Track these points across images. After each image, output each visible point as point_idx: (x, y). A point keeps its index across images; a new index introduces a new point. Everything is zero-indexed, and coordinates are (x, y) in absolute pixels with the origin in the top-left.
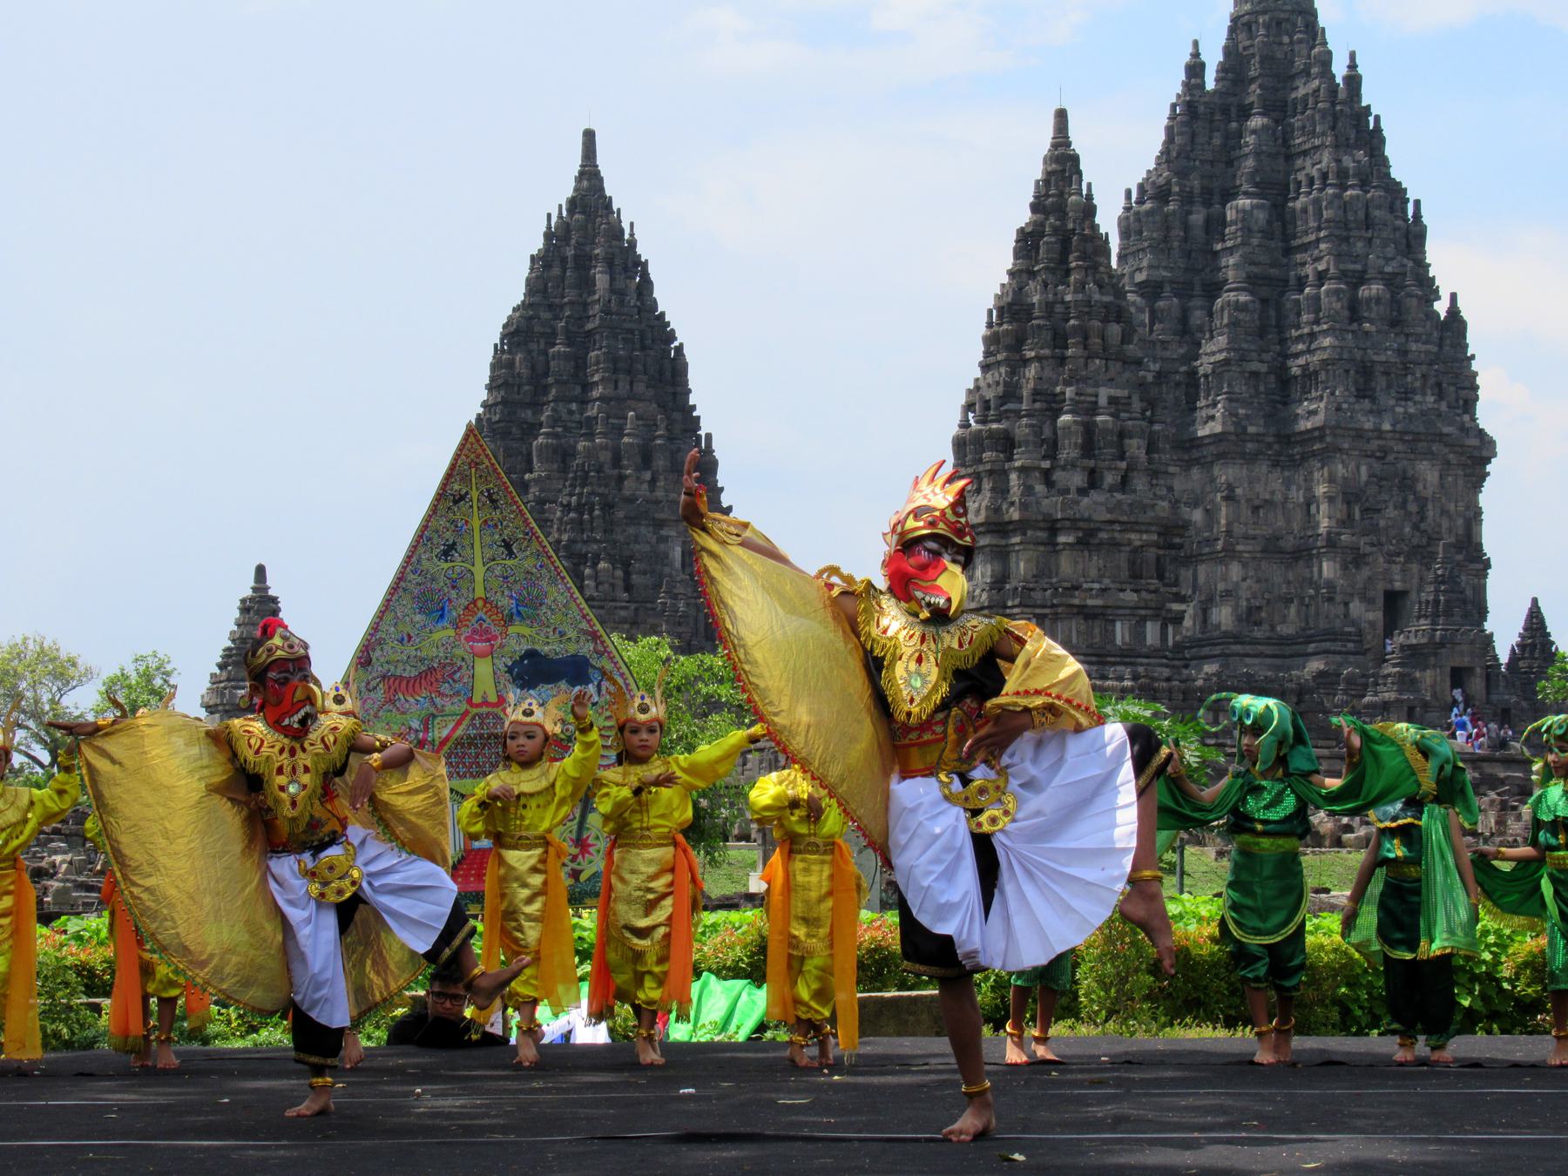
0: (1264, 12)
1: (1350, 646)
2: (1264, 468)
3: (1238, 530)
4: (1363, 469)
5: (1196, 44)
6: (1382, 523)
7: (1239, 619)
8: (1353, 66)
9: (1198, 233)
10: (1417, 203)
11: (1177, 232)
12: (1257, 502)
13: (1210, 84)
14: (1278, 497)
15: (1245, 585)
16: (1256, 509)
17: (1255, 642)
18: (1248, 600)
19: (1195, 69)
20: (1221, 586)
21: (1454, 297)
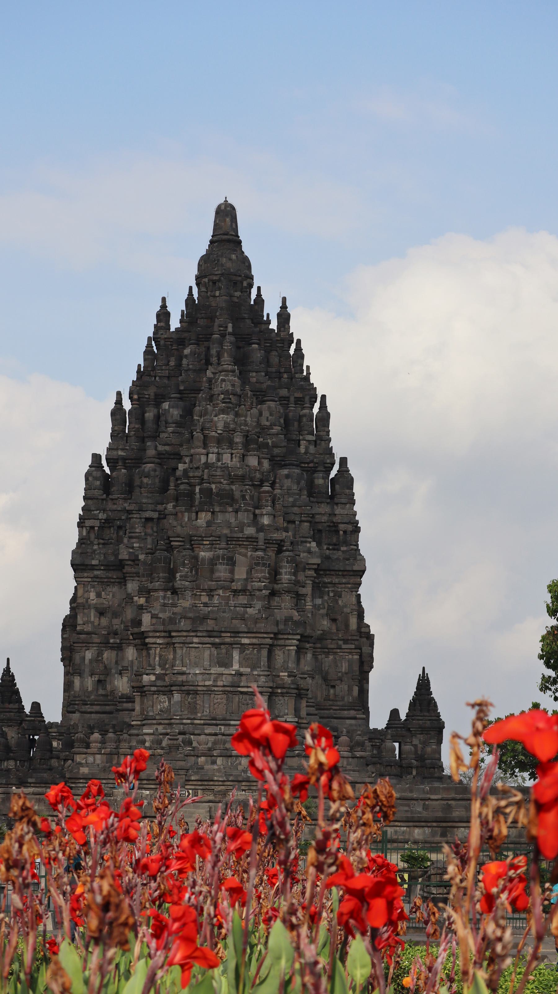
0: (205, 277)
5: (164, 299)
8: (284, 307)
9: (150, 425)
10: (324, 397)
13: (175, 323)
19: (163, 315)
21: (344, 461)
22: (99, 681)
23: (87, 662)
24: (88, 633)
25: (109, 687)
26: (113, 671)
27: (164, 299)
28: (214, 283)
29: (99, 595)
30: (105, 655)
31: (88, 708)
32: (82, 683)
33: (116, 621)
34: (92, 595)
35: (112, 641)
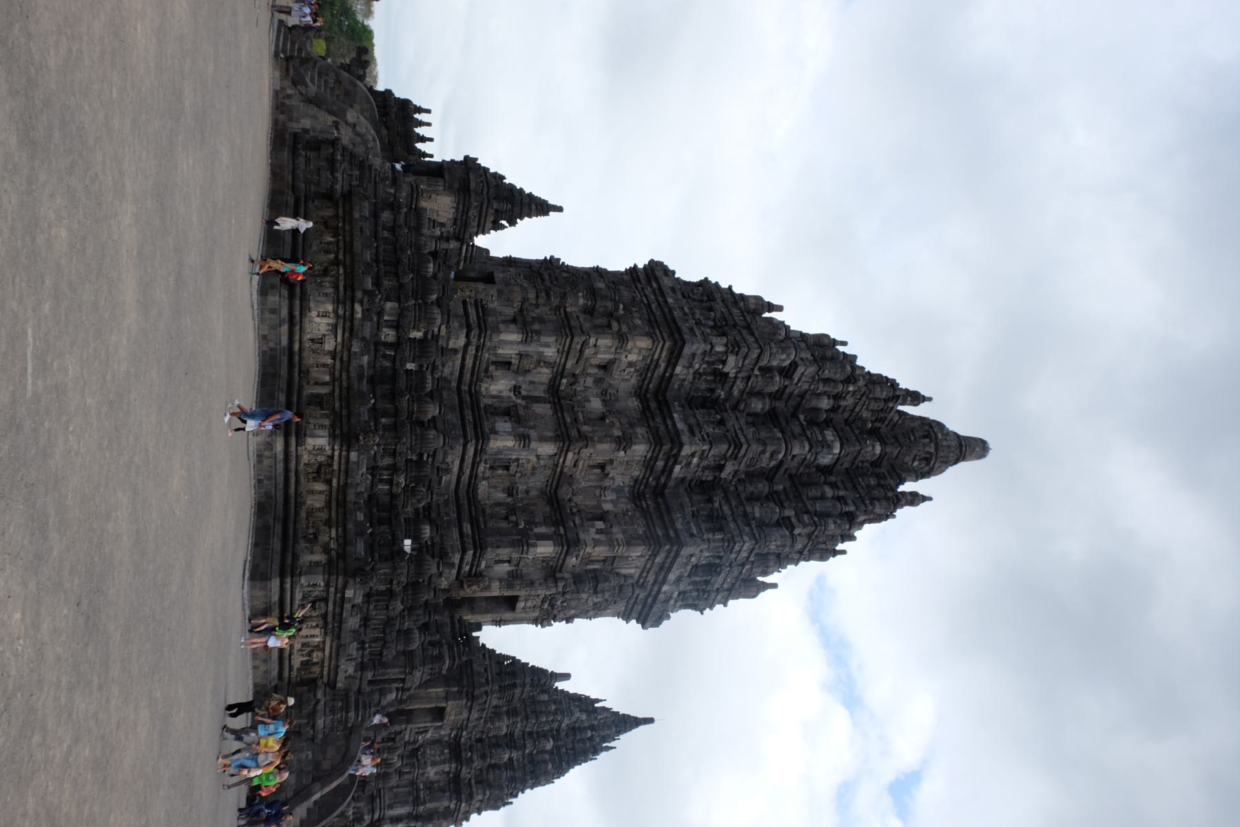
1: (467, 568)
2: (636, 473)
3: (586, 452)
4: (632, 571)
5: (930, 399)
6: (584, 596)
7: (499, 452)
11: (821, 388)
12: (608, 468)
14: (607, 483)
15: (534, 459)
16: (602, 467)
17: (475, 464)
18: (518, 460)
19: (916, 398)
20: (533, 433)
22: (509, 364)
23: (541, 349)
24: (581, 351)
25: (498, 373)
26: (521, 379)
27: (930, 399)
28: (927, 460)
29: (630, 364)
30: (545, 370)
31: (472, 351)
32: (511, 343)
33: (590, 381)
34: (633, 357)
35: (564, 381)
